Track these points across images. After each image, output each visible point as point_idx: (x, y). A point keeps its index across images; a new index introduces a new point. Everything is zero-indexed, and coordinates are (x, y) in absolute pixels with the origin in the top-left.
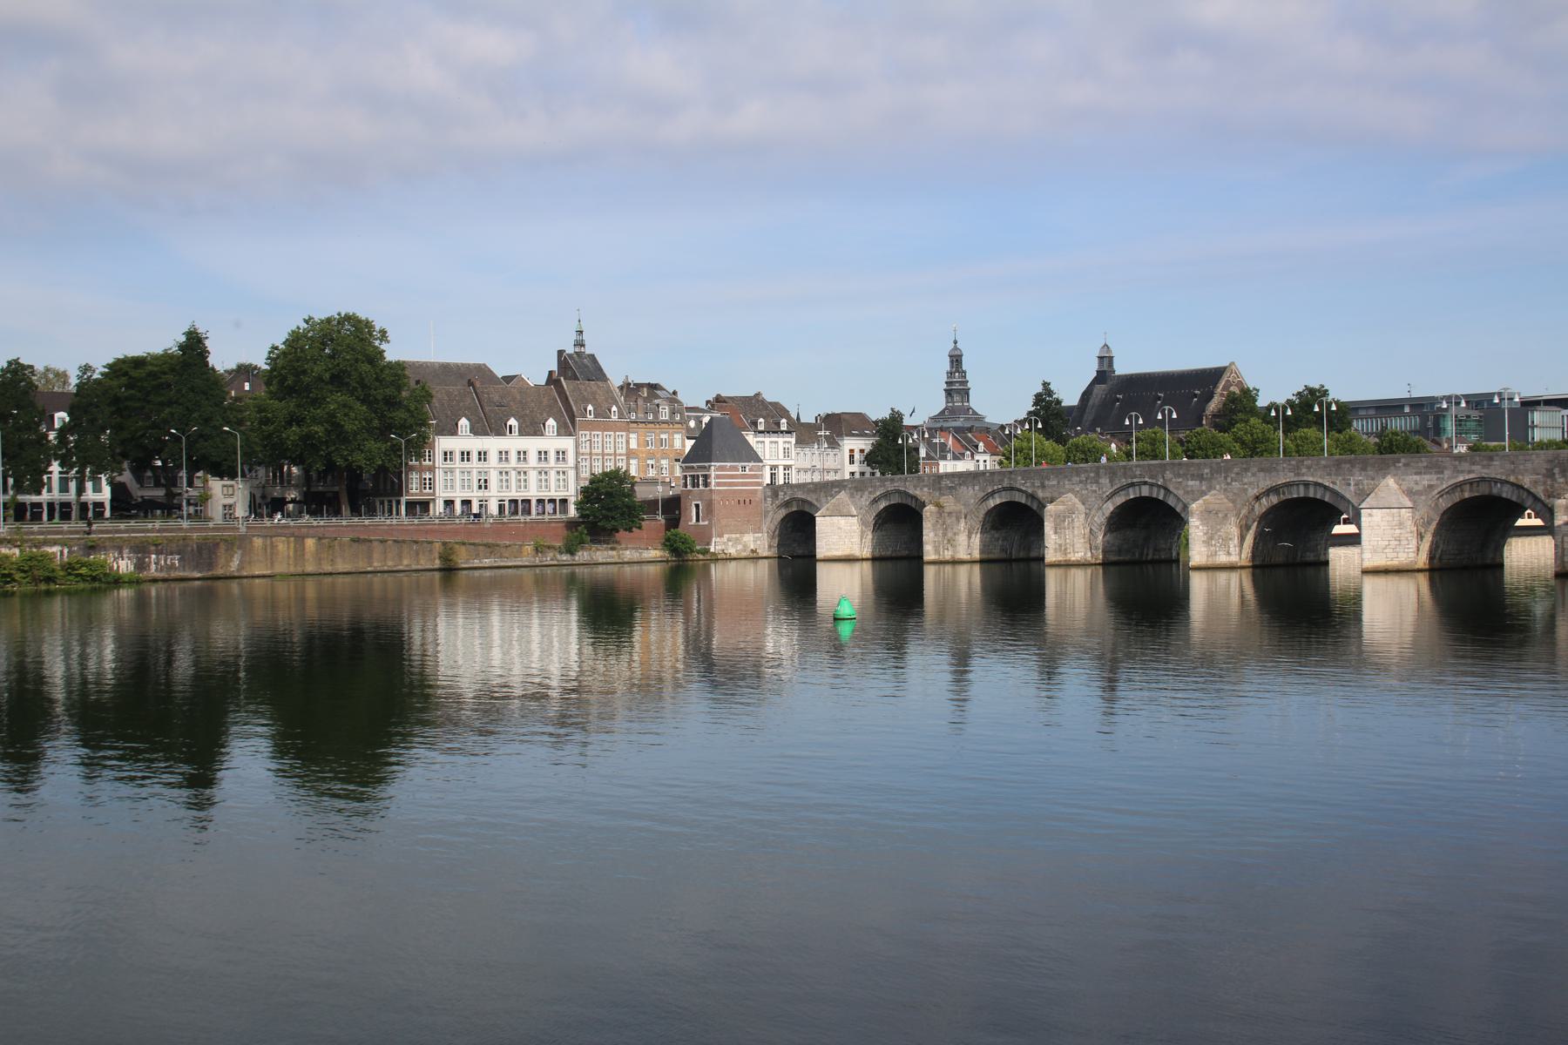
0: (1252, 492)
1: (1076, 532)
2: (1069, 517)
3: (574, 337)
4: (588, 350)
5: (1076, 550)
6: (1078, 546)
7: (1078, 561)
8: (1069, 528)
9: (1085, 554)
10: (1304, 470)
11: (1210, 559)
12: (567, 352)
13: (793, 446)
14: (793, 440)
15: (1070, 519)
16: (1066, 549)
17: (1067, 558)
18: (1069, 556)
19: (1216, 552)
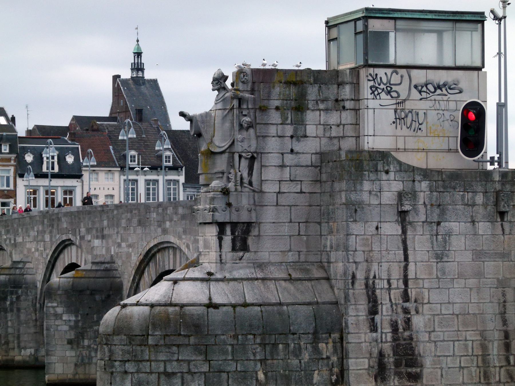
0: (135, 259)
1: (23, 317)
2: (12, 293)
3: (131, 59)
4: (148, 75)
5: (22, 344)
6: (25, 338)
7: (24, 361)
8: (12, 310)
9: (36, 351)
10: (168, 224)
11: (80, 370)
12: (122, 77)
13: (181, 188)
14: (182, 179)
15: (14, 297)
16: (7, 343)
17: (9, 358)
18: (12, 353)
19: (90, 358)
